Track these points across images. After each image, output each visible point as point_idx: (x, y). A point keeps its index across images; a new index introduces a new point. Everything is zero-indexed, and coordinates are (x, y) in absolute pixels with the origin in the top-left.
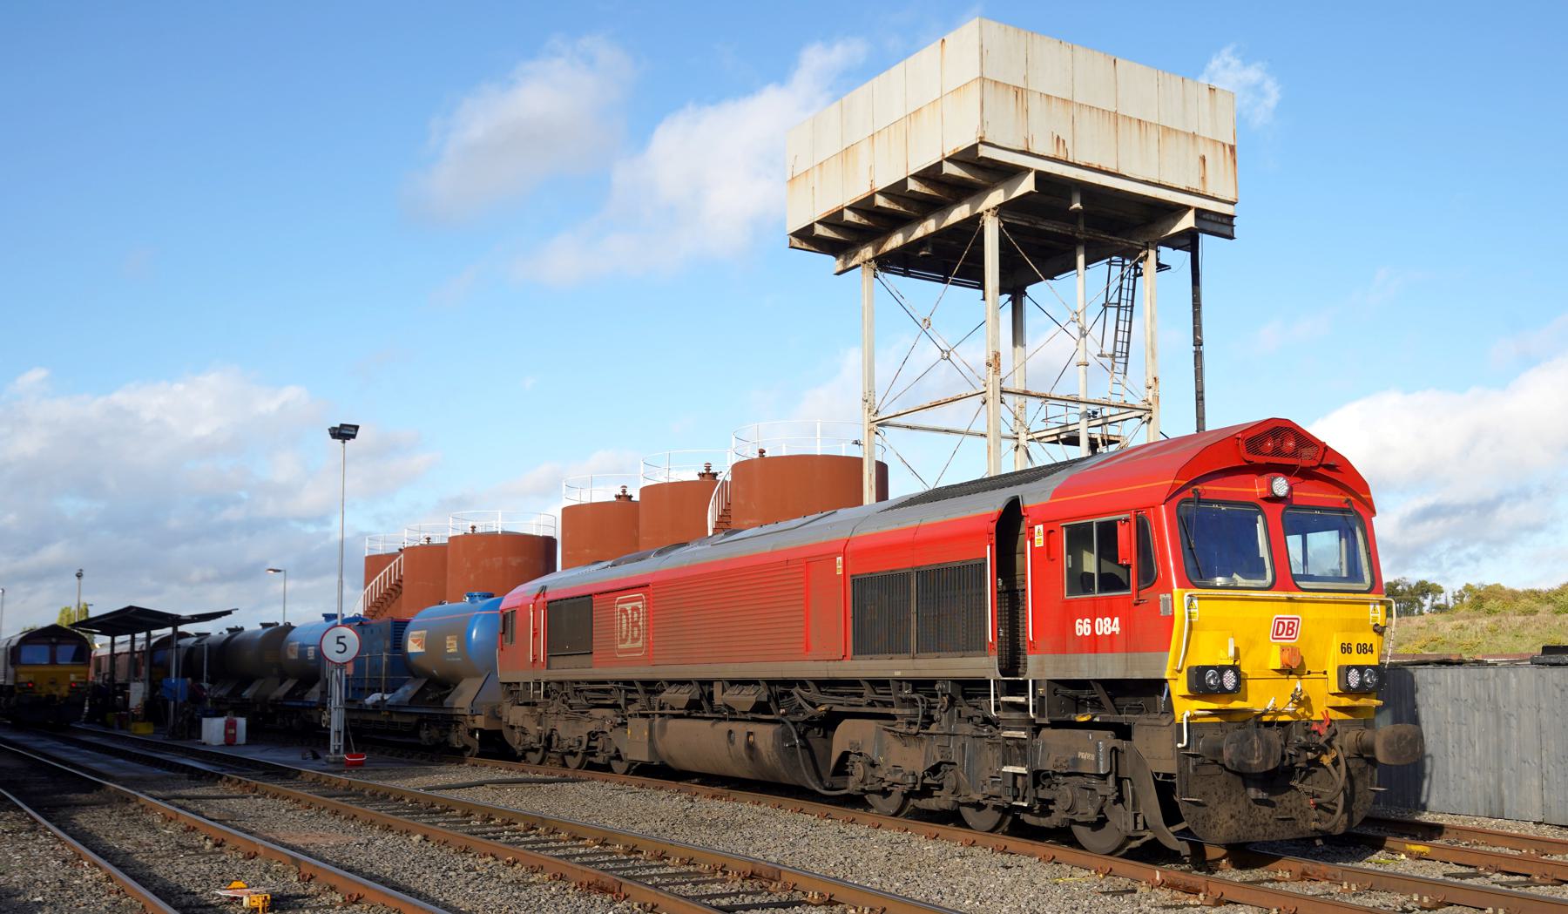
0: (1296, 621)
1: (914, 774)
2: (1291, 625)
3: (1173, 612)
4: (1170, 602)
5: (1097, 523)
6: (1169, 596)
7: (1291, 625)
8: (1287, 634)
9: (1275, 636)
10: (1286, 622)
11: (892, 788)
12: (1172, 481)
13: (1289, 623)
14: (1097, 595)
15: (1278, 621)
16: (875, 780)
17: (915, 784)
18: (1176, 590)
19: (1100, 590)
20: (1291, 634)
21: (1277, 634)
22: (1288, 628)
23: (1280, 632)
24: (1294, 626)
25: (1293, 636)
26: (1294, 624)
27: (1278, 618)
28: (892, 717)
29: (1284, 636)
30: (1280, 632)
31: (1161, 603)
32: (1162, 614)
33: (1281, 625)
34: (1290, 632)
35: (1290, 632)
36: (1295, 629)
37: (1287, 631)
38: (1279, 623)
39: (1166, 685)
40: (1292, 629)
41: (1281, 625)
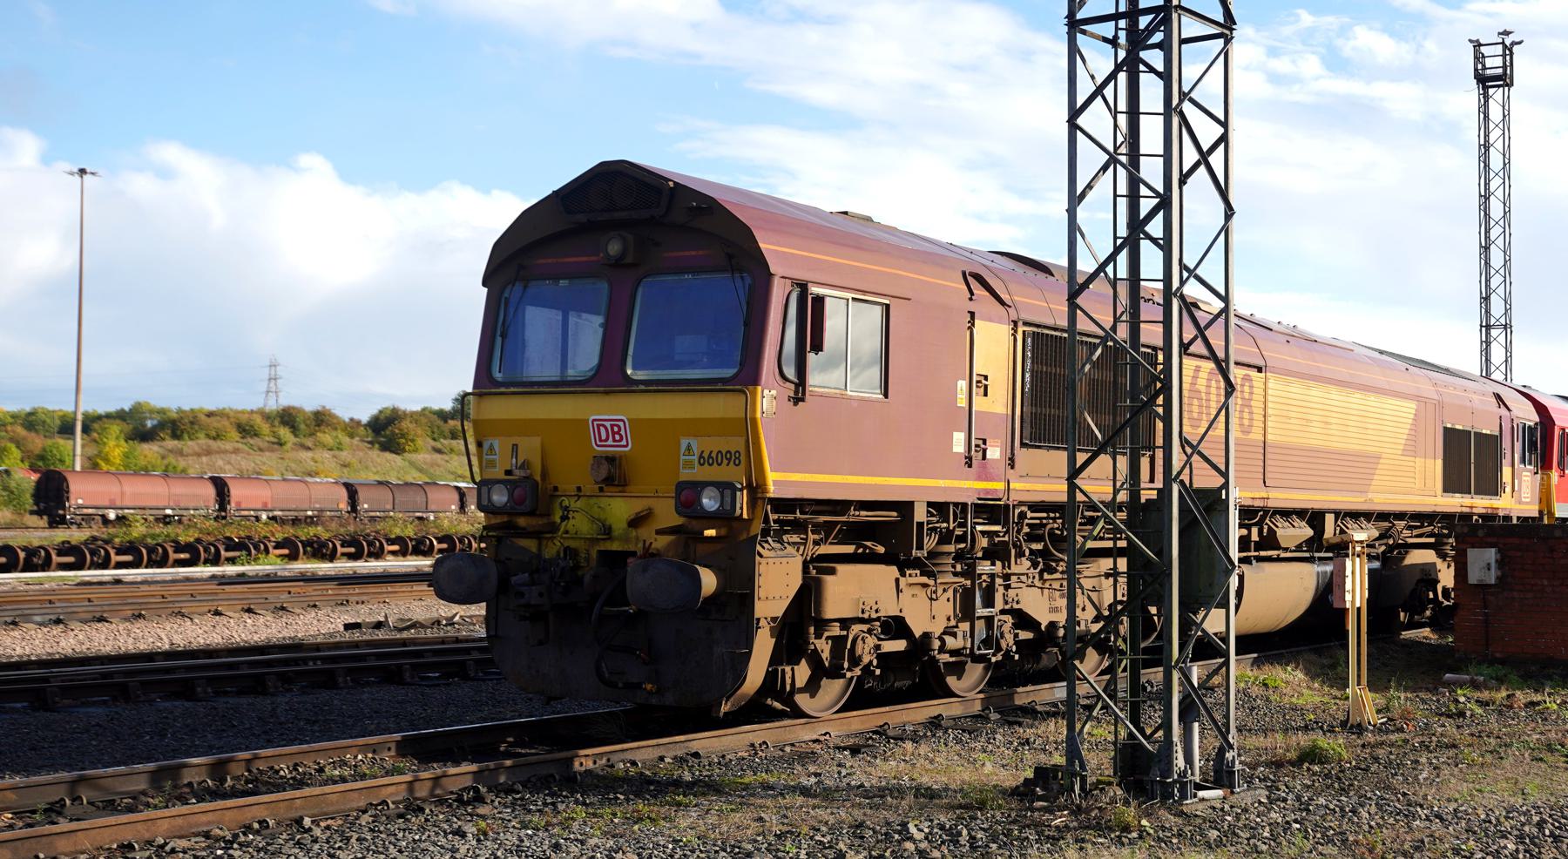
0: (621, 424)
2: (616, 429)
7: (616, 429)
8: (614, 440)
9: (599, 443)
10: (608, 424)
13: (612, 426)
15: (595, 423)
20: (621, 440)
21: (601, 440)
22: (614, 433)
23: (604, 437)
24: (620, 429)
25: (624, 443)
26: (618, 426)
27: (594, 420)
29: (610, 442)
30: (604, 437)
33: (602, 429)
34: (617, 437)
35: (617, 437)
36: (623, 432)
37: (614, 437)
38: (598, 426)
40: (618, 433)
41: (602, 429)
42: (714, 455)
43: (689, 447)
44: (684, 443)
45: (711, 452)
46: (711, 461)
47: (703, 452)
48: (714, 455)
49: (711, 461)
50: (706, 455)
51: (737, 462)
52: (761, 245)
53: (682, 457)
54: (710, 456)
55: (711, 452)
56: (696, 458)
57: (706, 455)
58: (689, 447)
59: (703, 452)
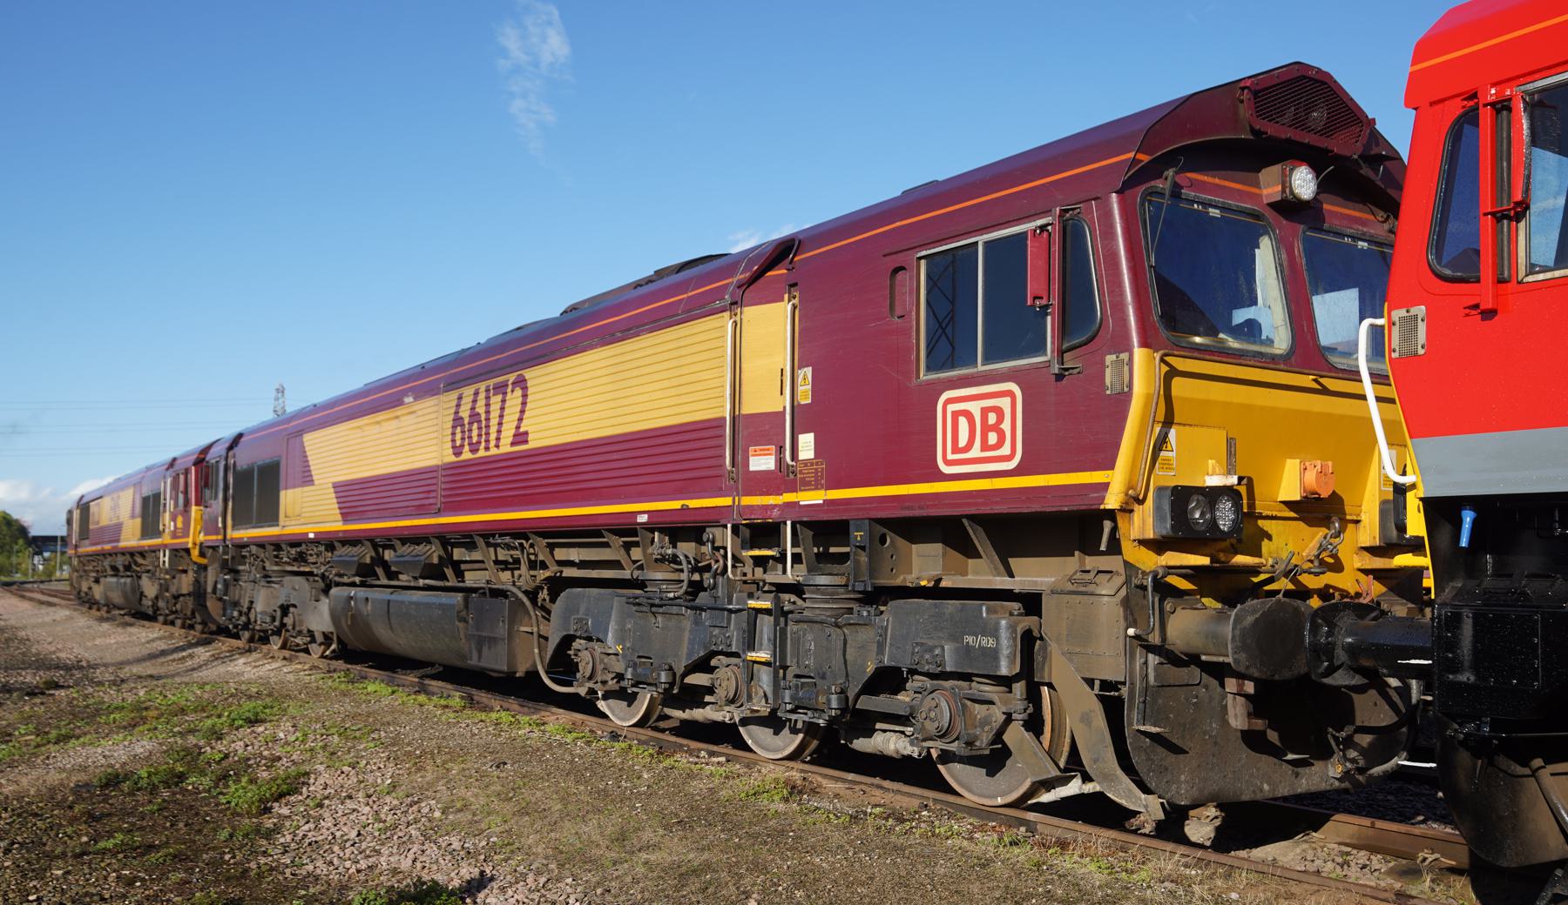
1: (671, 669)
3: (1130, 386)
4: (1126, 368)
5: (987, 244)
6: (1124, 356)
11: (635, 690)
12: (1131, 155)
14: (981, 368)
16: (609, 677)
17: (672, 684)
18: (1139, 354)
19: (988, 359)
28: (641, 584)
31: (1108, 372)
32: (1108, 392)
39: (1107, 525)
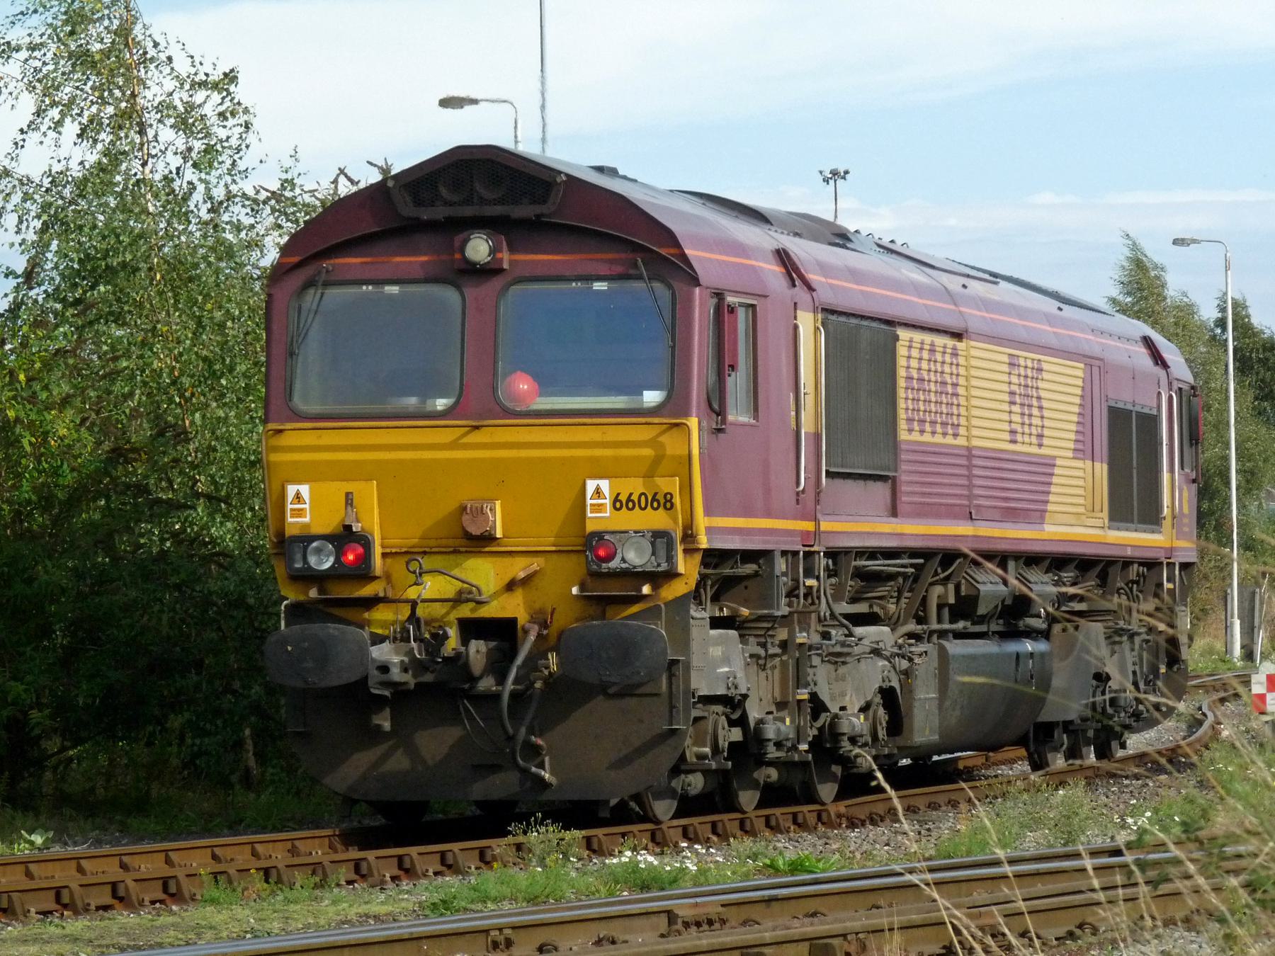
42: (635, 498)
43: (598, 492)
44: (591, 485)
45: (631, 494)
46: (630, 505)
47: (618, 494)
48: (635, 498)
49: (630, 505)
50: (623, 498)
51: (668, 505)
52: (687, 251)
53: (589, 502)
54: (629, 500)
55: (631, 494)
56: (607, 502)
57: (623, 498)
58: (598, 492)
59: (618, 494)
